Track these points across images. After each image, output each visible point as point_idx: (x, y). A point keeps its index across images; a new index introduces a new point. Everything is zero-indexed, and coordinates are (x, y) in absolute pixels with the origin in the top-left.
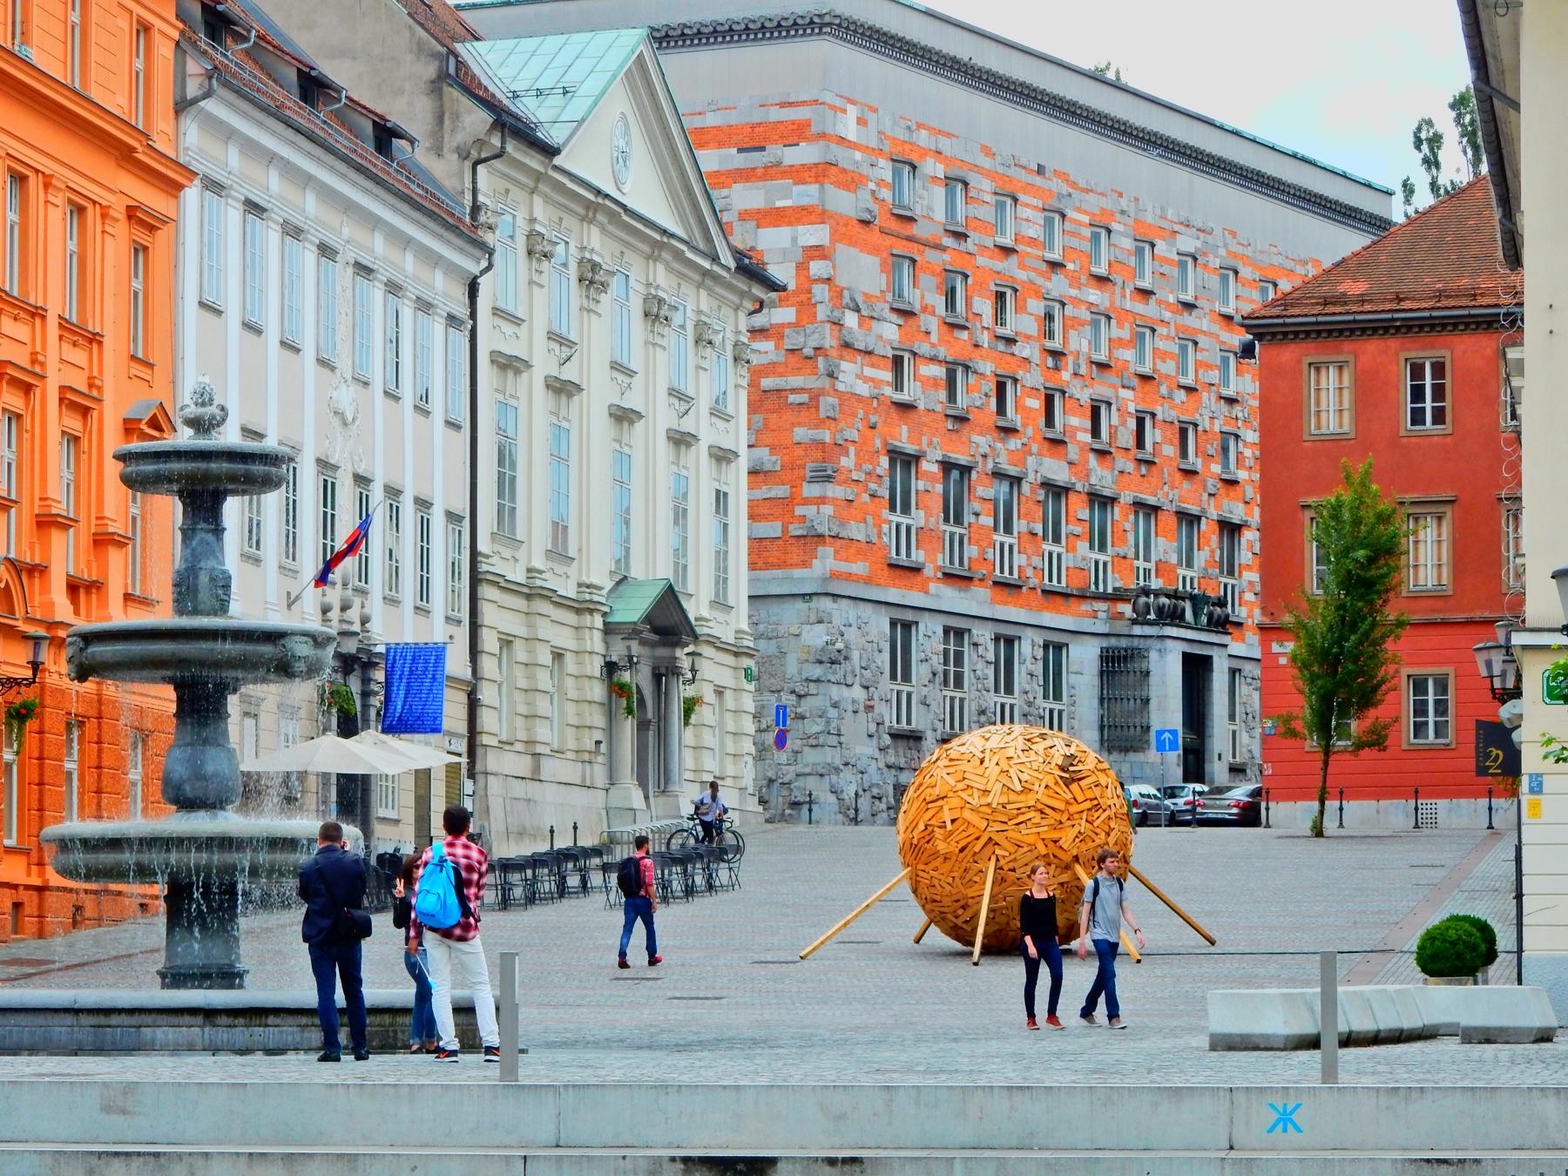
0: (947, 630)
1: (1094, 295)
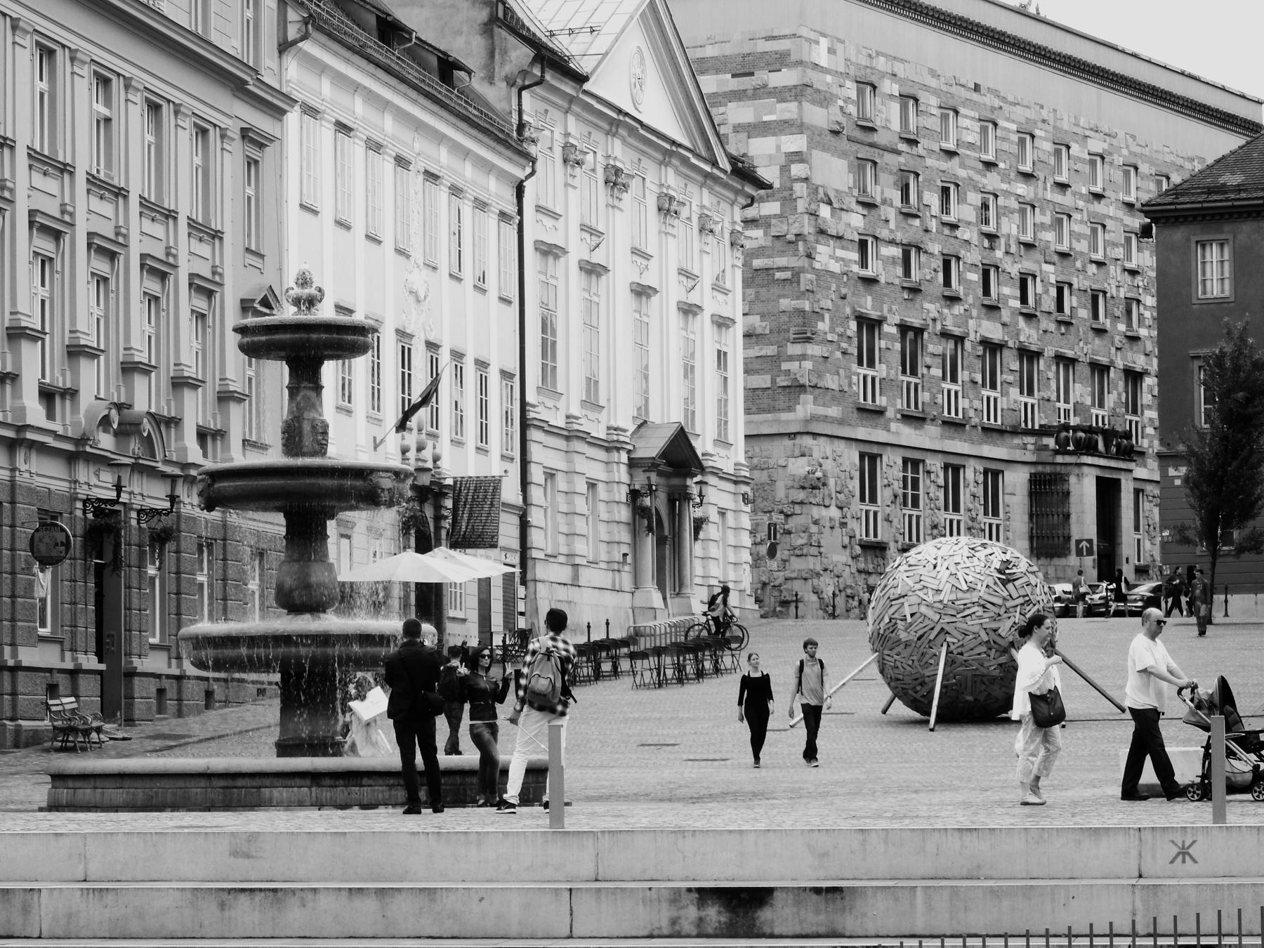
0: (905, 461)
1: (1021, 188)
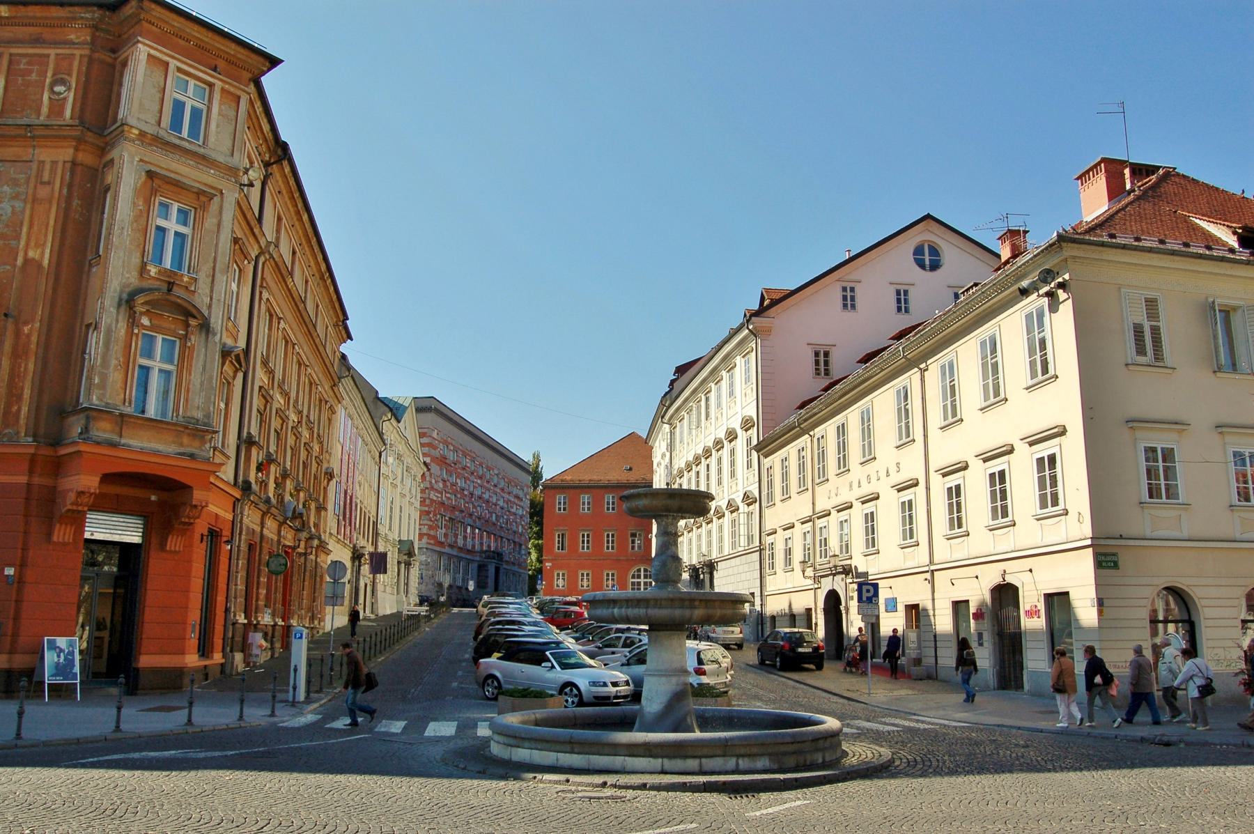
1: (479, 481)
